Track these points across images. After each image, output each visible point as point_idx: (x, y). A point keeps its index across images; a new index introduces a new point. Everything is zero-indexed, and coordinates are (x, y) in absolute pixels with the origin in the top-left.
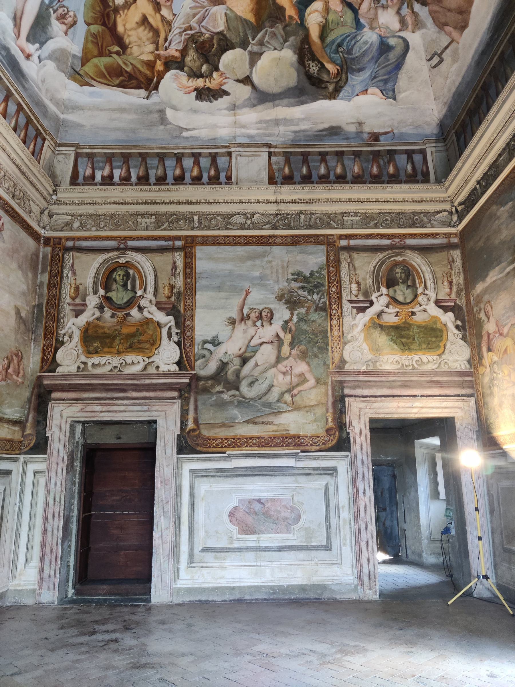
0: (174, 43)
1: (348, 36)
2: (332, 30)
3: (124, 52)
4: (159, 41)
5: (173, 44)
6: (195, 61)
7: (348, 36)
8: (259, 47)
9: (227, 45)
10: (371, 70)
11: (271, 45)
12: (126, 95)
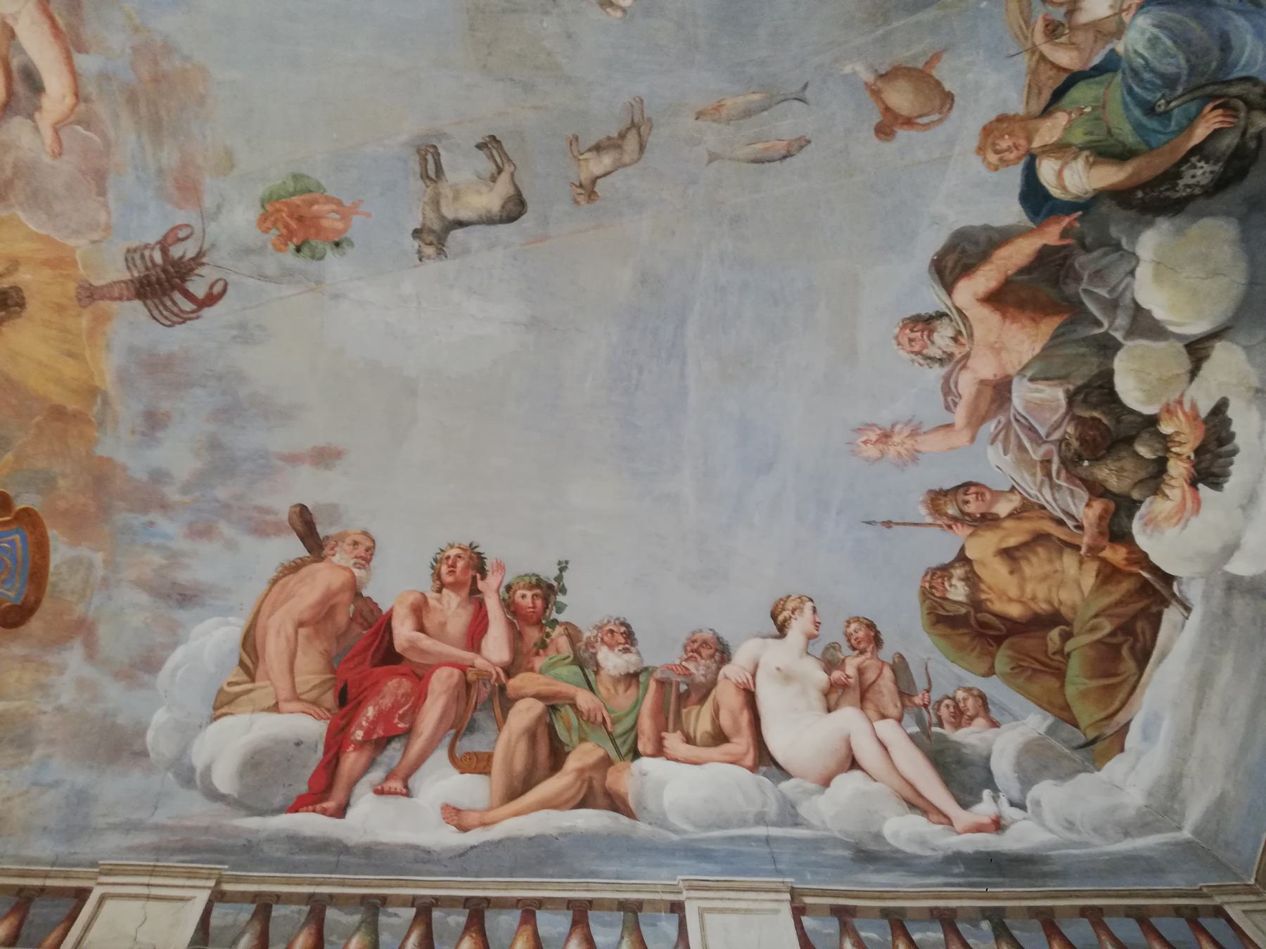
0: (1072, 507)
1: (1130, 91)
2: (1109, 132)
3: (1068, 623)
4: (1059, 539)
5: (1073, 510)
6: (1122, 469)
7: (1130, 91)
8: (1119, 312)
9: (1100, 387)
10: (1230, 13)
11: (1121, 282)
12: (1170, 657)
